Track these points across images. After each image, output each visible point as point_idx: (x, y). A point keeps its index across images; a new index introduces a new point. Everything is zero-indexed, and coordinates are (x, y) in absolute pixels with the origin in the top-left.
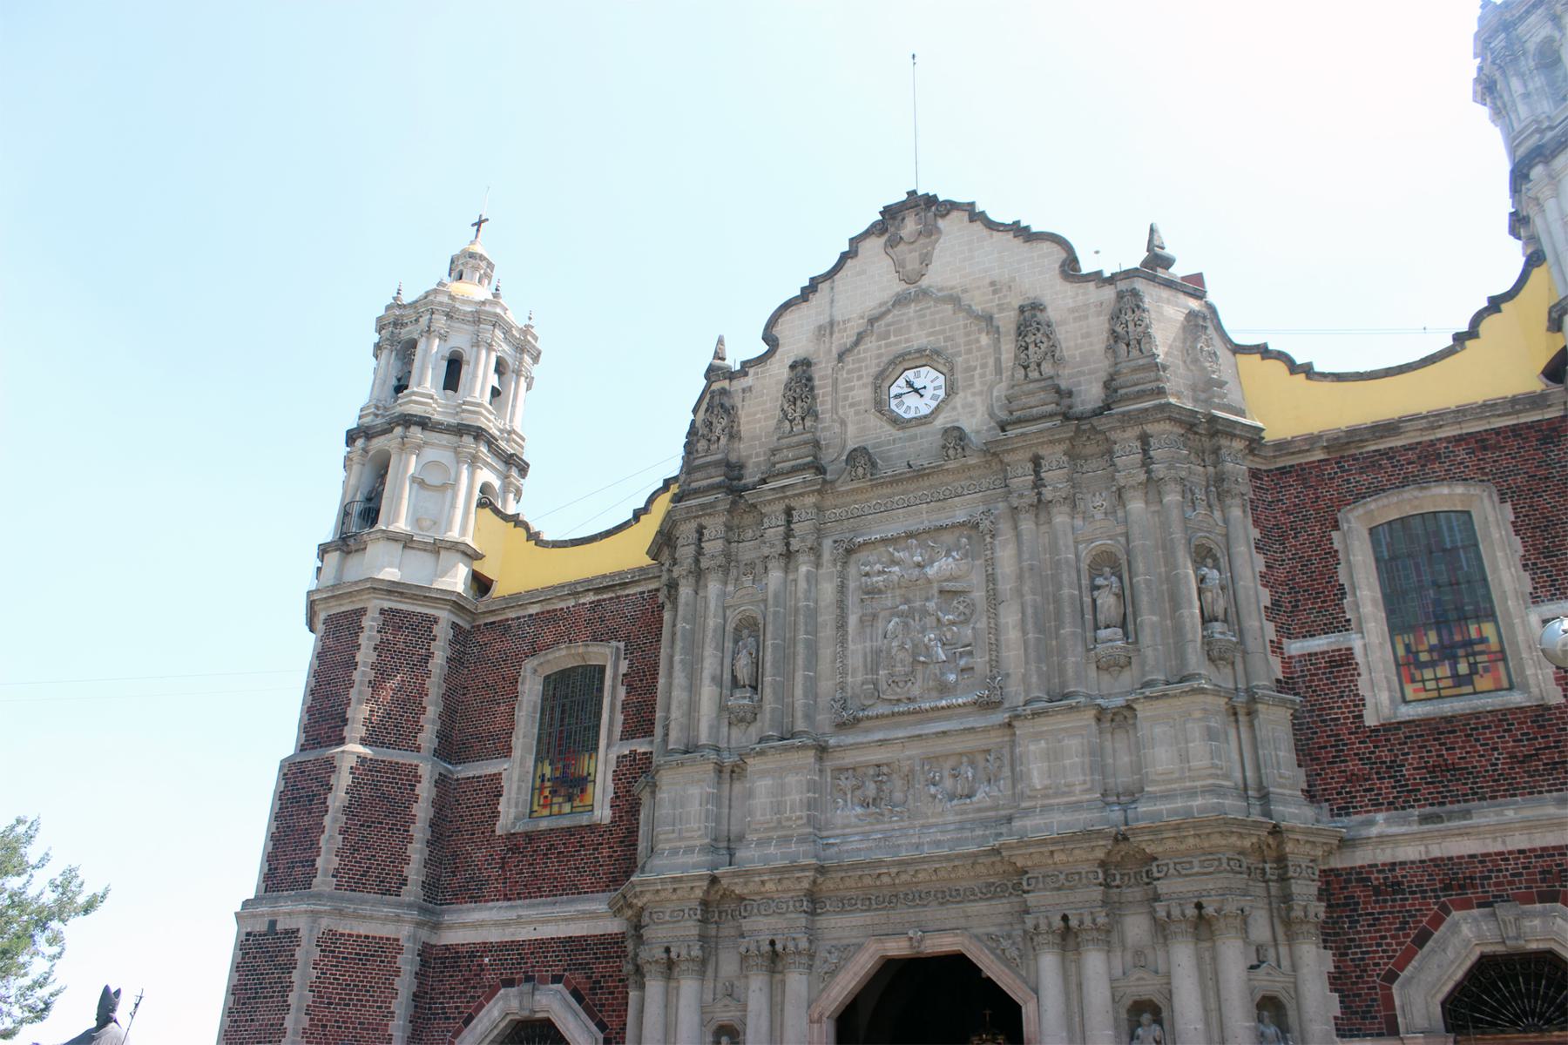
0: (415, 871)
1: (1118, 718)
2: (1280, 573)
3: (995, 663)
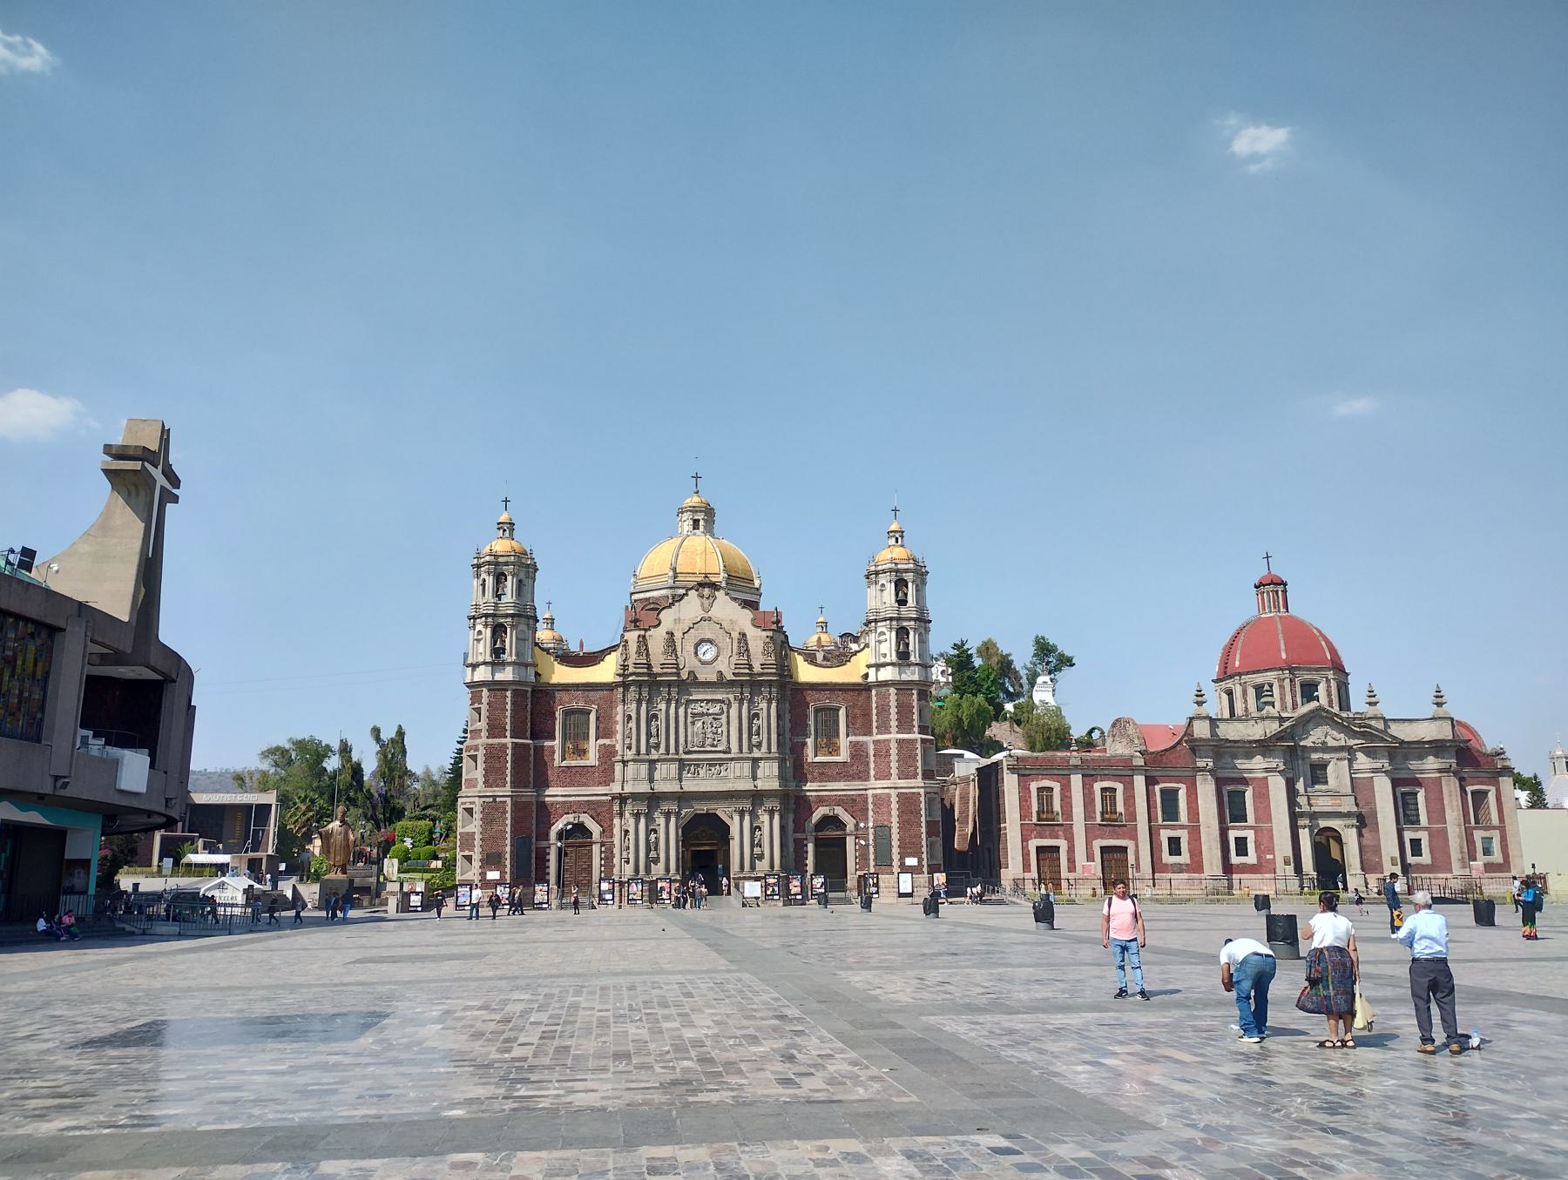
0: (531, 779)
1: (755, 761)
2: (793, 719)
3: (729, 742)
